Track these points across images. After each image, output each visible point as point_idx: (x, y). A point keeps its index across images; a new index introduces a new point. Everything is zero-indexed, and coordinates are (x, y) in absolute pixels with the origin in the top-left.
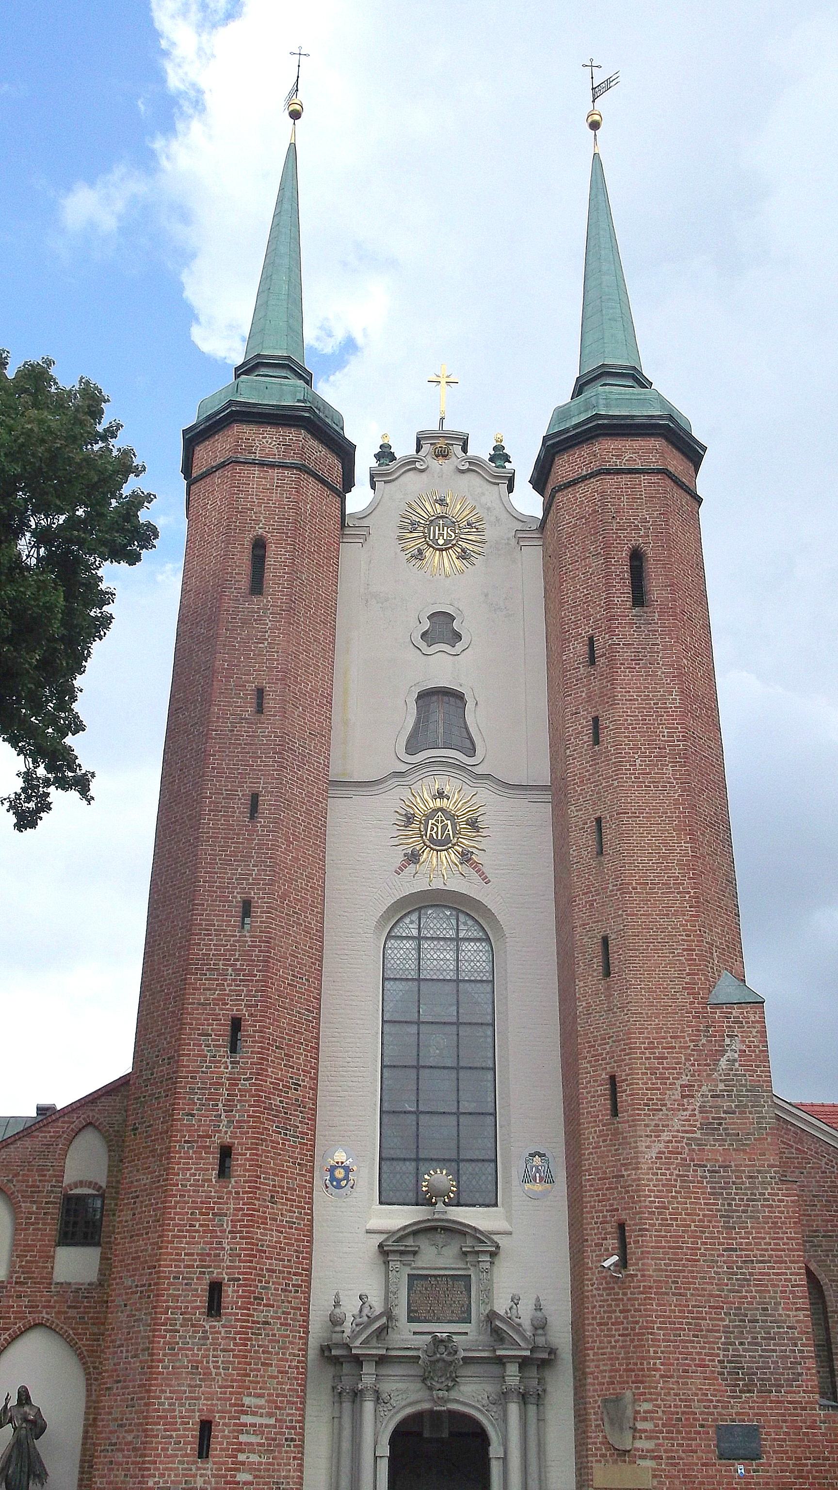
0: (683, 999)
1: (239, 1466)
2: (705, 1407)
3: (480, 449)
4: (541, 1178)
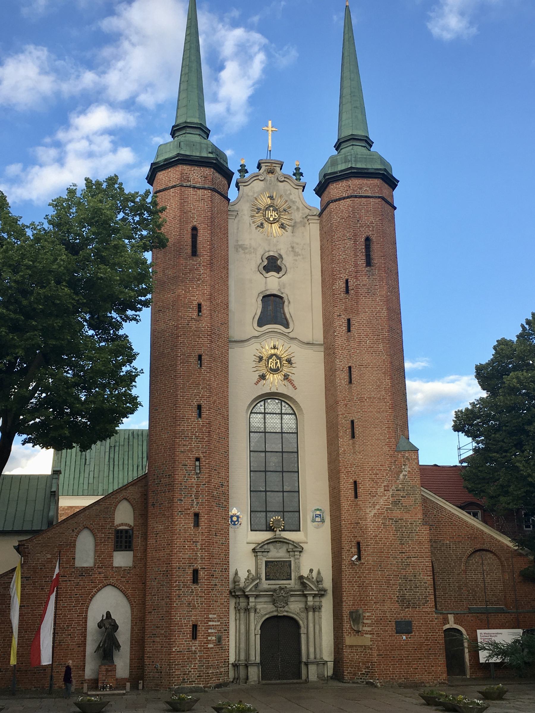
0: (386, 449)
1: (208, 642)
2: (391, 614)
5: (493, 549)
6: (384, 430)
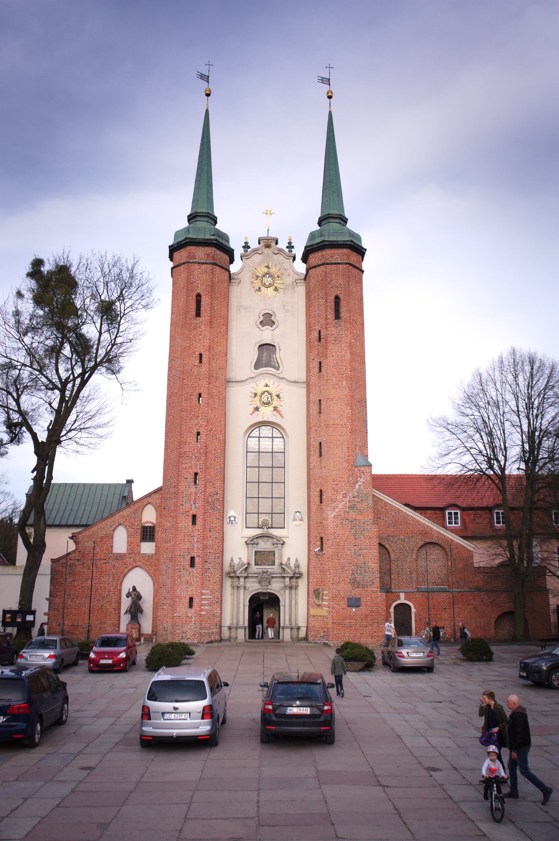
0: (346, 464)
1: (202, 610)
3: (283, 245)
4: (299, 520)
5: (440, 542)
6: (345, 450)
